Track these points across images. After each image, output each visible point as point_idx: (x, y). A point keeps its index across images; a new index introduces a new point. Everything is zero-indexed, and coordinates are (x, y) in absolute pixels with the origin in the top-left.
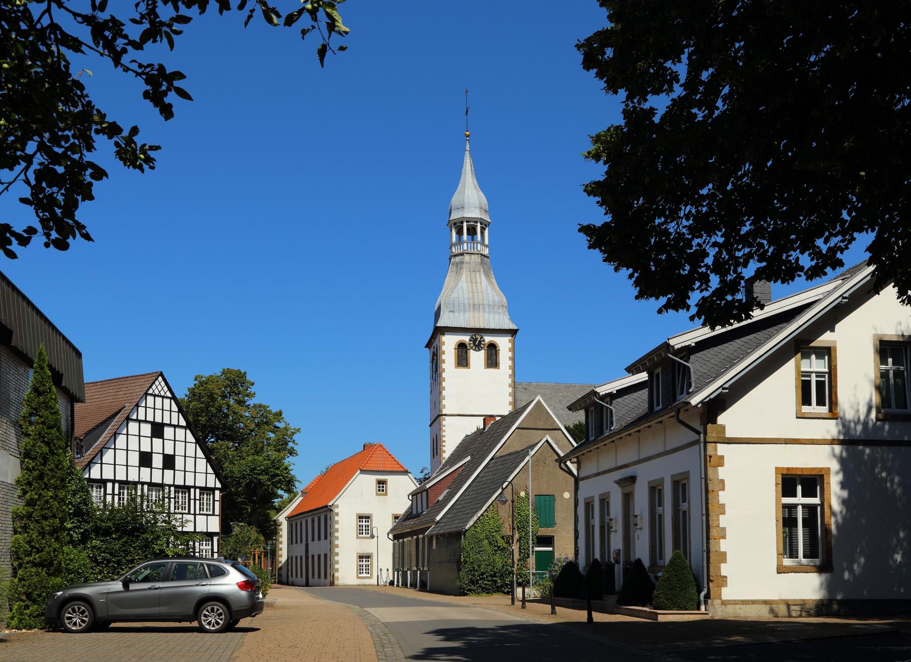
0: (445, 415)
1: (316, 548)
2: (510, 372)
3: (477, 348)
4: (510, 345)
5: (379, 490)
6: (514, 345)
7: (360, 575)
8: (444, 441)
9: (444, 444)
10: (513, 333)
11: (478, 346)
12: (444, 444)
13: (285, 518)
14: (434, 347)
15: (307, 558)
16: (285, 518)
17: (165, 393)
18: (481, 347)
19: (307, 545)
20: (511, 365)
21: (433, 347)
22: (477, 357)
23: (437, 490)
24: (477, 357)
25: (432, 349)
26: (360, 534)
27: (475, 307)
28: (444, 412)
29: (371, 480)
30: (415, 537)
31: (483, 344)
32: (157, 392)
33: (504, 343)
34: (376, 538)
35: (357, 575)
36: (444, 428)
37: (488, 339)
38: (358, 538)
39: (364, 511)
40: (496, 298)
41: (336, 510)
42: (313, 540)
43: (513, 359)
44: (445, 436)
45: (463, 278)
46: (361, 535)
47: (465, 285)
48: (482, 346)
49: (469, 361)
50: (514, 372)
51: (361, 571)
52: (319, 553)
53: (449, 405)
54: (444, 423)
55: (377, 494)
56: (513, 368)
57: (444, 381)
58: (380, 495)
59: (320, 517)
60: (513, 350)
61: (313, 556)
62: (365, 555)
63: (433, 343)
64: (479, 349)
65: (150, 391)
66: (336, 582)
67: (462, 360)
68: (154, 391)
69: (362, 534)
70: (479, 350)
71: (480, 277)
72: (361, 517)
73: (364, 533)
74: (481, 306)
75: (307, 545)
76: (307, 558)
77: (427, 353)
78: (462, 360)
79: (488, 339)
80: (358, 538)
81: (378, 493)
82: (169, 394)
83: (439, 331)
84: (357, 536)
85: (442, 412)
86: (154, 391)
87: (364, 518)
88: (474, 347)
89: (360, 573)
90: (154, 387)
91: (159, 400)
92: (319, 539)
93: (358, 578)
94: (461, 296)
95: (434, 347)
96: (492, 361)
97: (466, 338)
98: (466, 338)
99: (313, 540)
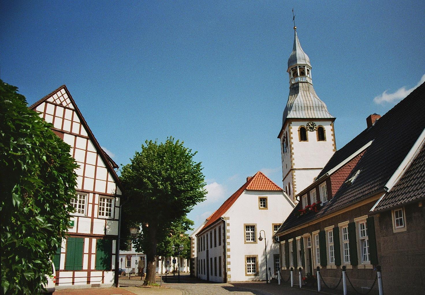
0: (295, 169)
1: (215, 252)
2: (333, 142)
3: (312, 130)
4: (331, 127)
5: (261, 206)
6: (333, 127)
7: (248, 273)
8: (296, 185)
9: (295, 186)
10: (333, 120)
11: (312, 129)
12: (295, 186)
13: (195, 235)
14: (284, 134)
15: (208, 261)
16: (195, 235)
17: (68, 105)
18: (314, 129)
19: (207, 251)
20: (333, 138)
21: (283, 134)
22: (312, 135)
23: (339, 178)
24: (312, 135)
25: (282, 137)
26: (247, 240)
27: (308, 108)
28: (294, 167)
29: (255, 198)
30: (316, 233)
31: (315, 127)
32: (58, 102)
33: (328, 129)
34: (264, 240)
35: (246, 273)
36: (295, 177)
37: (318, 124)
38: (245, 243)
39: (250, 222)
40: (320, 103)
41: (227, 222)
42: (211, 247)
43: (334, 135)
44: (295, 182)
45: (300, 94)
46: (248, 241)
47: (301, 97)
48: (315, 128)
49: (308, 137)
50: (335, 142)
51: (249, 270)
52: (215, 257)
53: (297, 163)
54: (294, 174)
55: (260, 209)
56: (334, 140)
57: (293, 149)
58: (262, 209)
59: (216, 229)
60: (333, 130)
61: (211, 259)
62: (252, 256)
63: (283, 132)
64: (313, 130)
65: (51, 100)
66: (228, 280)
67: (303, 137)
68: (55, 100)
69: (249, 239)
70: (313, 131)
71: (309, 93)
72: (247, 227)
73: (250, 239)
74: (312, 108)
75: (207, 251)
76: (208, 261)
77: (279, 141)
78: (303, 137)
79: (318, 124)
80: (245, 243)
81: (261, 207)
82: (71, 106)
83: (287, 122)
84: (245, 241)
85: (293, 167)
86: (55, 100)
87: (251, 227)
88: (310, 129)
89: (248, 272)
90: (55, 96)
91: (60, 110)
92: (215, 246)
93: (247, 275)
94: (299, 102)
95: (284, 134)
96: (321, 136)
97: (304, 124)
98: (304, 124)
99: (211, 247)
